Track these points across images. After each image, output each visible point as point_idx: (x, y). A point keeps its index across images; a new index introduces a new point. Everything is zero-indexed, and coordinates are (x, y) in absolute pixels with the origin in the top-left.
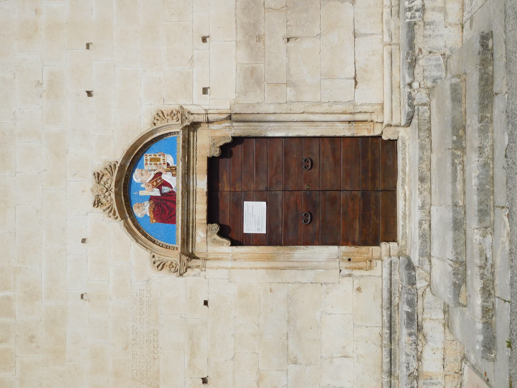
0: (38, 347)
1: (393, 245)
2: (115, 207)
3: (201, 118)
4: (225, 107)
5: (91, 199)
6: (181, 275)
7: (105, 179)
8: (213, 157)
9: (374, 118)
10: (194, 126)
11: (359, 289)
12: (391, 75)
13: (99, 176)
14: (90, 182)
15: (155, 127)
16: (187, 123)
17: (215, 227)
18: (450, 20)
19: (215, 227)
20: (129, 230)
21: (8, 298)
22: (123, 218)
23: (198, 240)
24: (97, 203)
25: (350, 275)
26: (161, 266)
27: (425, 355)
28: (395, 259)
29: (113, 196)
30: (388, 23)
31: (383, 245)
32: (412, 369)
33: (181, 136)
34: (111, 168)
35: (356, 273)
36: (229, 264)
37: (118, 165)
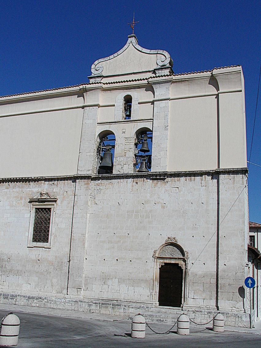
0: (139, 224)
1: (158, 305)
2: (168, 242)
3: (187, 263)
4: (188, 268)
5: (170, 237)
6: (153, 257)
7: (174, 240)
8: (179, 264)
9: (185, 302)
10: (185, 261)
11: (148, 296)
12: (194, 307)
13: (174, 238)
14: (173, 236)
15: (185, 251)
16: (186, 259)
17: (164, 264)
18: (202, 320)
19: (164, 264)
20: (163, 245)
21: (149, 218)
22: (165, 244)
23: (161, 260)
24: (169, 238)
25: (151, 294)
26: (155, 252)
27: (133, 309)
28: (154, 305)
29: (170, 242)
30: (206, 307)
31: (158, 303)
32: (130, 306)
33: (183, 257)
34: (176, 241)
35: (152, 296)
36: (155, 268)
37: (177, 243)
